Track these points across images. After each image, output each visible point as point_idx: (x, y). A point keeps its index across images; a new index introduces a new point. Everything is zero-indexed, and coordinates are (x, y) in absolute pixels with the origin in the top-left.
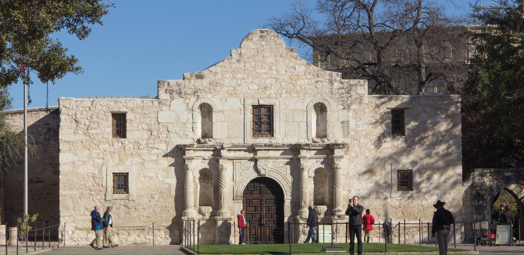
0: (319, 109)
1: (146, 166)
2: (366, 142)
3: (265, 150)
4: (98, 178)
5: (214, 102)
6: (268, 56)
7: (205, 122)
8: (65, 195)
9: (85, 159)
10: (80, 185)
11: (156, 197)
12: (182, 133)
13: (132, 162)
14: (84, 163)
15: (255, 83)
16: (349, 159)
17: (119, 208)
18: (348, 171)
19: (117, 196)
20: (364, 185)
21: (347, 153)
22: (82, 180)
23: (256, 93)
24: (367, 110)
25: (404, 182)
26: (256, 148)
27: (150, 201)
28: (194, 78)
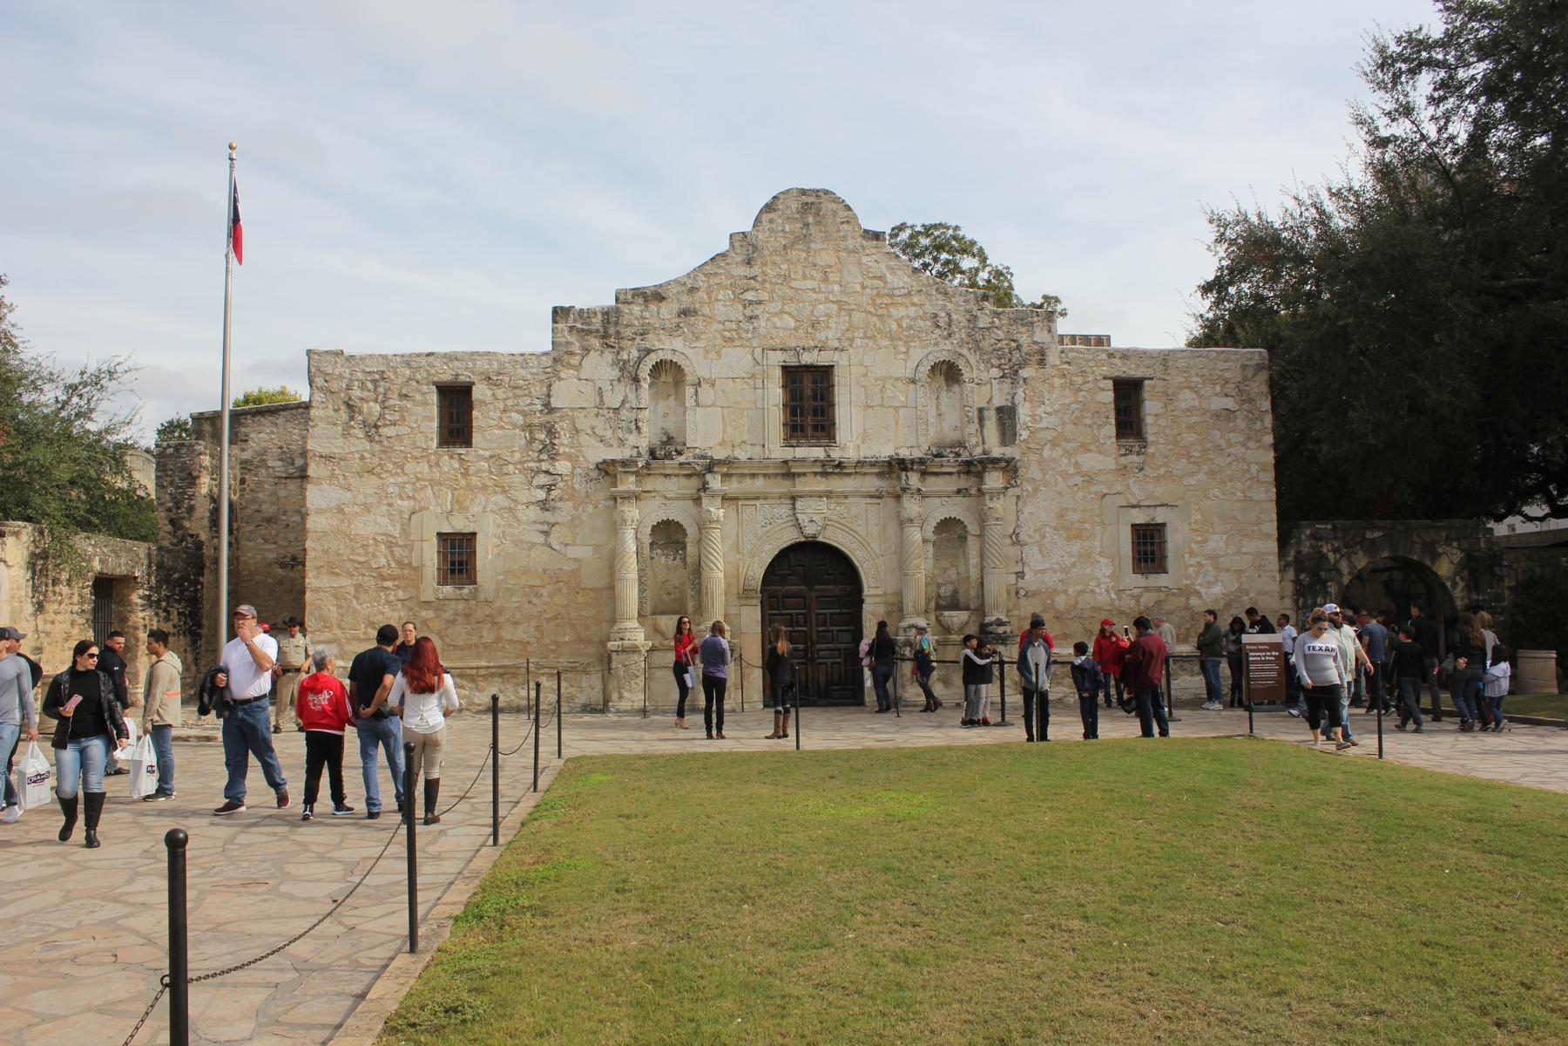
1: (519, 515)
2: (1055, 456)
3: (816, 474)
4: (400, 546)
5: (691, 356)
6: (819, 250)
7: (669, 408)
8: (317, 590)
9: (370, 500)
10: (356, 565)
11: (545, 592)
12: (609, 433)
13: (485, 507)
14: (367, 508)
15: (789, 314)
16: (1018, 497)
17: (453, 622)
18: (1017, 526)
19: (448, 590)
20: (1054, 561)
21: (1013, 482)
22: (362, 551)
23: (790, 335)
24: (1057, 381)
25: (1146, 553)
26: (793, 470)
27: (530, 602)
28: (641, 301)
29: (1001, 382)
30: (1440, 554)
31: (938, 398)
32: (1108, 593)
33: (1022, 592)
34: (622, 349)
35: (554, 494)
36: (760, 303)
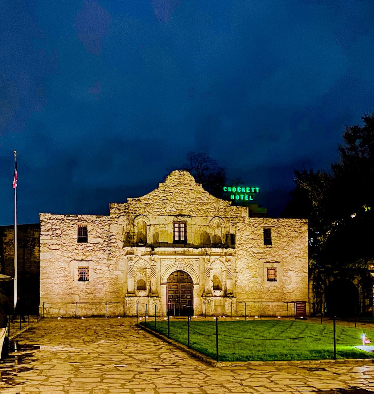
0: (216, 225)
18: (236, 267)
29: (232, 227)
30: (355, 278)
31: (215, 231)
32: (260, 286)
33: (237, 286)
34: (129, 216)
35: (110, 256)
36: (167, 203)
